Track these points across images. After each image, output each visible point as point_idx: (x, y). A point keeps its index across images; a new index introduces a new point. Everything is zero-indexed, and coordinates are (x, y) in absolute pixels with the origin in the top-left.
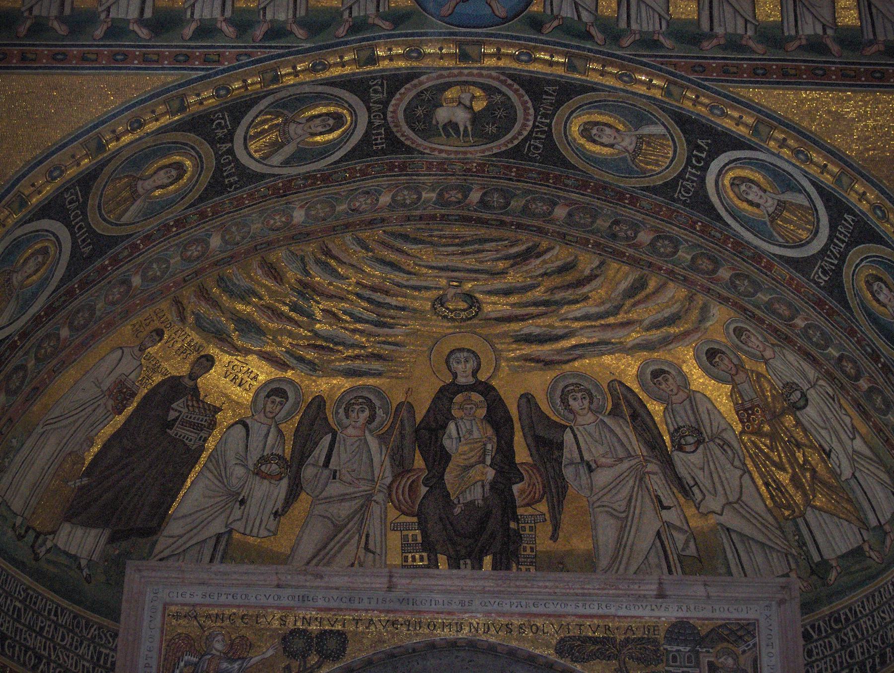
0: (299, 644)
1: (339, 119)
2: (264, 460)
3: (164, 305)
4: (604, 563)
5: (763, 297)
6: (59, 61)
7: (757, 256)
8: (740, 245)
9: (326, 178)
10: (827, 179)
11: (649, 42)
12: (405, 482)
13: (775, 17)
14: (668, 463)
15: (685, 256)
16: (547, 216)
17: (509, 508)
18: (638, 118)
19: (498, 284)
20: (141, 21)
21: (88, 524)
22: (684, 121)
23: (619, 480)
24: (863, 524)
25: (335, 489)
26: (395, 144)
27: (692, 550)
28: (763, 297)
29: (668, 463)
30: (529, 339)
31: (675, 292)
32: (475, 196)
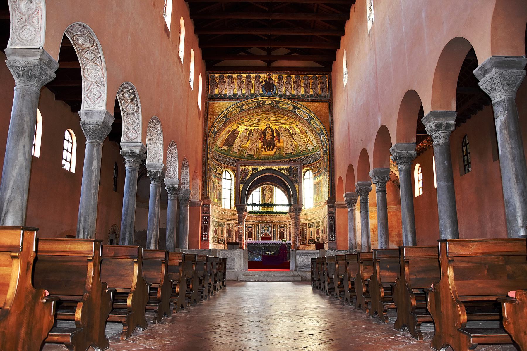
0: (253, 169)
1: (254, 104)
2: (245, 136)
3: (234, 122)
4: (285, 147)
5: (302, 122)
6: (223, 100)
7: (302, 118)
8: (299, 117)
9: (252, 109)
10: (309, 113)
11: (289, 97)
12: (261, 138)
13: (303, 93)
14: (292, 137)
15: (293, 117)
16: (278, 112)
17: (274, 141)
18: (288, 105)
19: (272, 117)
20: (232, 95)
21: (225, 146)
22: (292, 105)
23: (286, 138)
24: (314, 146)
25: (253, 139)
26: (260, 106)
27: (295, 146)
28: (302, 122)
29: (292, 137)
30: (276, 123)
31: (293, 120)
32: (269, 110)
